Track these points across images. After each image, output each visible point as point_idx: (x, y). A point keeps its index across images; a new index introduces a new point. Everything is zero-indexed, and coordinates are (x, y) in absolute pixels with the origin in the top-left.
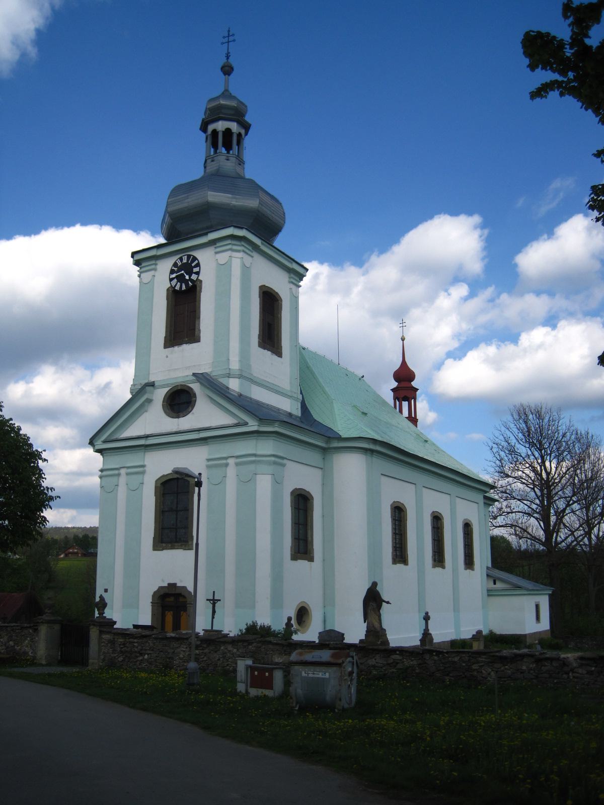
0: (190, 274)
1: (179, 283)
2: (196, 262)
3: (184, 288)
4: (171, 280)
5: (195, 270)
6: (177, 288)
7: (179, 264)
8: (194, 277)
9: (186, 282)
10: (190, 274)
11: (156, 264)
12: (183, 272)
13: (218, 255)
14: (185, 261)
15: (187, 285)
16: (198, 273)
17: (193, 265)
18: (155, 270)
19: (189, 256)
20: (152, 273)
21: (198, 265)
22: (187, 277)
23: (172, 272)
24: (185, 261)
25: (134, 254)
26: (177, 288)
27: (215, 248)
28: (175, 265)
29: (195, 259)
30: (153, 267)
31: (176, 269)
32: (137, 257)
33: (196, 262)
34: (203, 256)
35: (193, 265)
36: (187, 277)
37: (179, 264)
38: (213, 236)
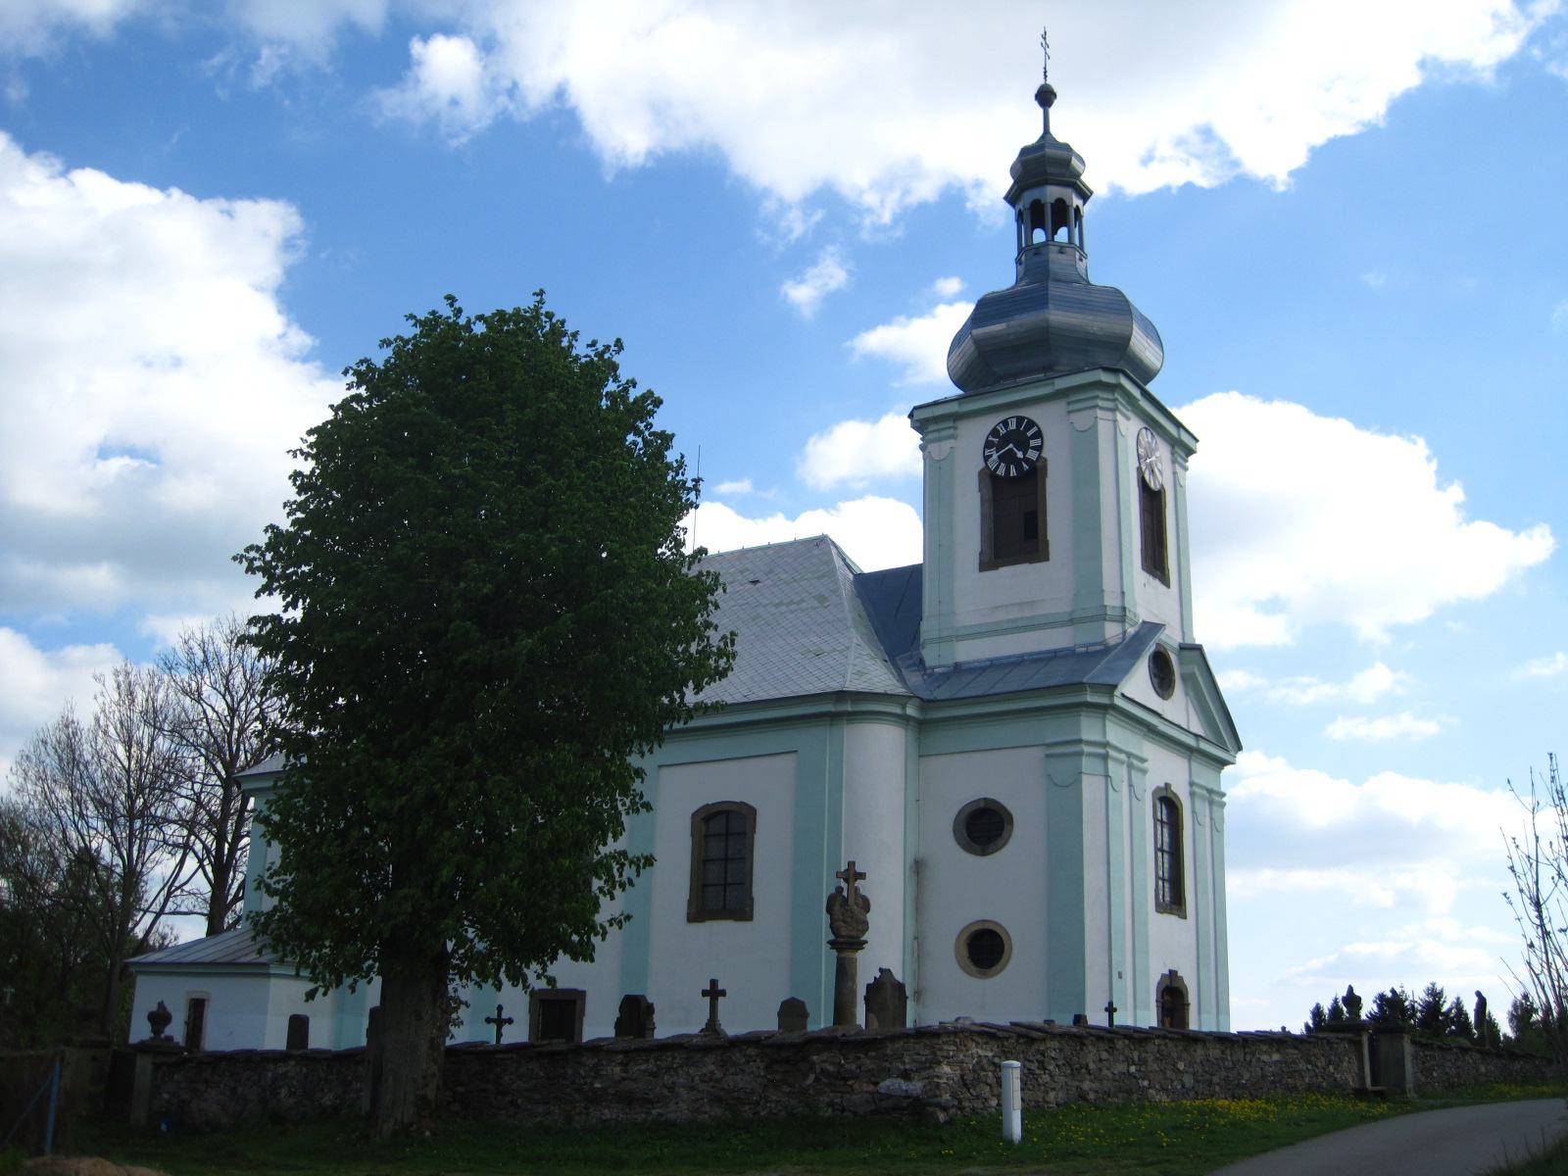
0: (1025, 449)
1: (1002, 464)
2: (1035, 429)
3: (1013, 472)
4: (986, 458)
5: (1033, 443)
6: (1001, 471)
7: (1003, 431)
8: (1032, 455)
9: (1018, 463)
10: (1025, 449)
11: (955, 428)
12: (1011, 446)
13: (1074, 417)
14: (1013, 426)
15: (1019, 468)
16: (1039, 448)
17: (1029, 434)
18: (953, 437)
19: (1020, 419)
20: (947, 445)
21: (1039, 435)
22: (1020, 455)
23: (988, 445)
24: (1013, 426)
26: (1001, 471)
27: (1069, 403)
28: (994, 432)
29: (1031, 424)
30: (951, 431)
31: (996, 440)
32: (918, 415)
33: (1035, 429)
34: (1050, 420)
35: (1029, 434)
36: (1020, 455)
37: (1003, 431)
38: (1062, 383)
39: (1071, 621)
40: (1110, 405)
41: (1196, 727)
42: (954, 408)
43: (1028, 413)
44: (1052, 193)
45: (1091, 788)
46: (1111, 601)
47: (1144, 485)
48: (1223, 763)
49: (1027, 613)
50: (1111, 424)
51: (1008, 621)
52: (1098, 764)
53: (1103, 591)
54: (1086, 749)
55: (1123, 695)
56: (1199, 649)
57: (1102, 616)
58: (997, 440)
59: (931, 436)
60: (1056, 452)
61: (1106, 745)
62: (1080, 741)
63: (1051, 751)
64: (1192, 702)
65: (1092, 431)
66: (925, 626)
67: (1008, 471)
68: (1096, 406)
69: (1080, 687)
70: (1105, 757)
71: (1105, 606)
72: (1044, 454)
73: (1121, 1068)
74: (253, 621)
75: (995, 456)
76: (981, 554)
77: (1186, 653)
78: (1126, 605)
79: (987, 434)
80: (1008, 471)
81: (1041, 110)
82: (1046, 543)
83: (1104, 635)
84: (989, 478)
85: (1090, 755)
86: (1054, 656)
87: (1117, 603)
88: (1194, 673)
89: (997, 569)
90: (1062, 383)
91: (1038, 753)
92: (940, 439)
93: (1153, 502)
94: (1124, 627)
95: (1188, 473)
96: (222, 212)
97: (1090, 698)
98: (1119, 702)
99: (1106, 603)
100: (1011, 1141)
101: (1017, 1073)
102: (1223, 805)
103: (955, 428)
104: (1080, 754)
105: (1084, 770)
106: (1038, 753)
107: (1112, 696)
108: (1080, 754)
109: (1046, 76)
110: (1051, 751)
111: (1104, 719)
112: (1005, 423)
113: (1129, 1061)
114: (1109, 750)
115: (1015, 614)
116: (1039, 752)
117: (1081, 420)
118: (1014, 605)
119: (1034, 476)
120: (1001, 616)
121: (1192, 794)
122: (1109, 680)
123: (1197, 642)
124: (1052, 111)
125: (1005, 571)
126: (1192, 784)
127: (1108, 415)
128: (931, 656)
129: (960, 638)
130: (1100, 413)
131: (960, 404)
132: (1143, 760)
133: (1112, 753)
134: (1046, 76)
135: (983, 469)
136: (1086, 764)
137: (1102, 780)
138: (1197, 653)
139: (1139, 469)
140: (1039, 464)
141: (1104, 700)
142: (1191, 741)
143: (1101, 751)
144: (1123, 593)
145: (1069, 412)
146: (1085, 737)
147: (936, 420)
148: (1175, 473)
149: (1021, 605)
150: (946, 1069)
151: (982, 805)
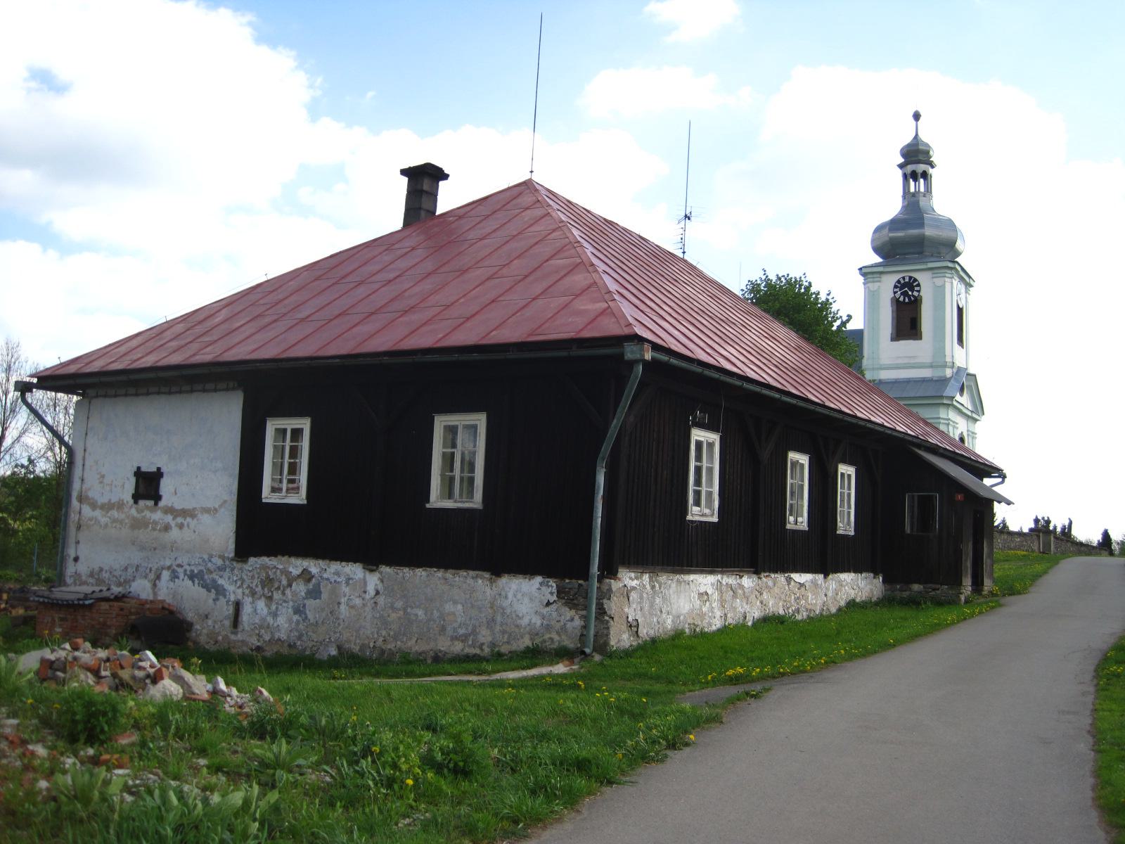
0: (913, 291)
3: (907, 300)
4: (895, 293)
5: (916, 289)
6: (901, 299)
7: (902, 282)
8: (916, 294)
9: (909, 297)
10: (913, 291)
14: (907, 280)
15: (910, 299)
16: (919, 291)
17: (914, 284)
18: (880, 281)
19: (910, 278)
20: (878, 284)
21: (919, 285)
22: (910, 293)
23: (895, 287)
24: (907, 280)
25: (860, 269)
26: (901, 299)
27: (933, 274)
28: (899, 282)
29: (915, 280)
30: (879, 279)
31: (899, 285)
32: (864, 270)
33: (917, 282)
34: (924, 279)
35: (914, 284)
36: (910, 293)
37: (902, 282)
38: (931, 265)
40: (949, 275)
42: (881, 269)
44: (921, 168)
46: (948, 359)
48: (976, 420)
49: (912, 361)
51: (905, 364)
54: (942, 421)
57: (945, 366)
58: (900, 285)
61: (949, 419)
62: (939, 418)
65: (943, 286)
66: (865, 362)
67: (904, 299)
68: (945, 277)
69: (942, 397)
70: (948, 424)
75: (899, 293)
77: (969, 377)
80: (904, 299)
81: (914, 122)
85: (943, 423)
90: (931, 265)
92: (874, 282)
93: (960, 311)
97: (945, 402)
98: (955, 403)
102: (976, 438)
103: (880, 277)
104: (940, 423)
108: (940, 423)
112: (904, 278)
115: (906, 361)
117: (938, 282)
119: (916, 303)
120: (900, 361)
121: (968, 435)
125: (902, 342)
126: (968, 431)
130: (947, 279)
132: (957, 424)
133: (951, 423)
138: (974, 377)
140: (919, 298)
141: (950, 402)
142: (969, 413)
143: (947, 422)
144: (953, 356)
145: (933, 278)
148: (966, 298)
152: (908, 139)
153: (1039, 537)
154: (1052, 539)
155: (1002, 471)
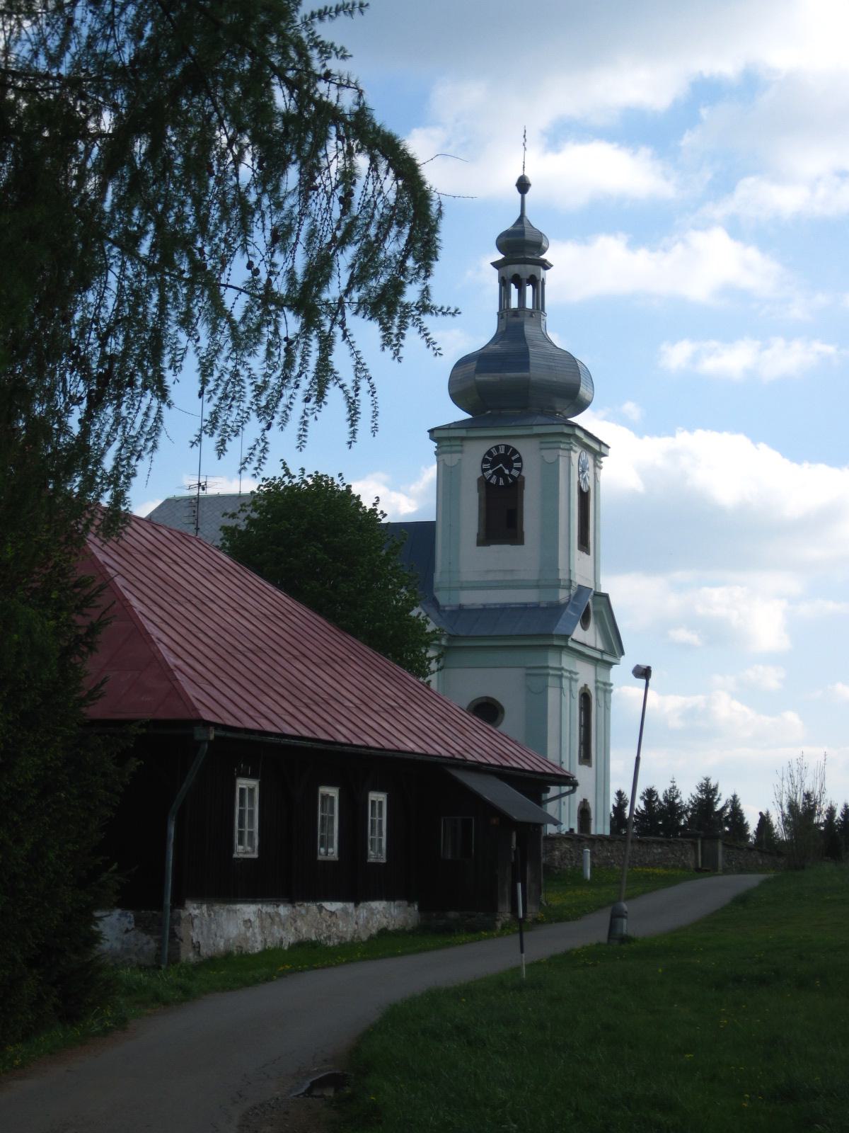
0: (510, 468)
1: (495, 476)
2: (517, 456)
3: (501, 482)
4: (484, 470)
5: (516, 465)
7: (495, 454)
8: (515, 473)
10: (510, 468)
11: (462, 446)
12: (501, 465)
13: (544, 453)
14: (502, 451)
15: (506, 480)
16: (520, 469)
17: (513, 458)
18: (461, 452)
19: (507, 447)
20: (457, 456)
21: (519, 460)
22: (507, 472)
23: (485, 461)
24: (502, 451)
25: (431, 431)
26: (493, 481)
27: (542, 443)
28: (489, 453)
29: (515, 452)
32: (437, 434)
33: (517, 456)
34: (526, 449)
35: (513, 458)
36: (507, 472)
38: (537, 430)
39: (538, 587)
40: (567, 447)
41: (600, 646)
42: (463, 433)
43: (515, 444)
44: (525, 270)
45: (552, 694)
46: (562, 575)
47: (580, 490)
48: (610, 665)
49: (509, 577)
50: (566, 459)
51: (497, 581)
52: (556, 681)
53: (558, 569)
54: (551, 672)
55: (572, 639)
56: (606, 596)
57: (556, 585)
58: (491, 460)
59: (444, 449)
60: (531, 472)
61: (562, 669)
62: (547, 667)
63: (530, 672)
64: (599, 632)
65: (556, 463)
66: (438, 577)
67: (498, 481)
68: (560, 448)
69: (551, 636)
70: (561, 677)
71: (560, 580)
72: (523, 473)
73: (605, 854)
74: (111, 622)
75: (490, 472)
76: (478, 535)
77: (597, 598)
78: (572, 579)
79: (485, 453)
80: (498, 481)
81: (520, 195)
82: (522, 533)
83: (558, 597)
84: (484, 484)
85: (553, 675)
86: (525, 608)
87: (566, 577)
88: (602, 612)
89: (489, 545)
90: (537, 430)
91: (522, 672)
92: (451, 452)
93: (584, 497)
94: (570, 592)
95: (602, 471)
96: (162, 421)
97: (556, 643)
98: (571, 644)
99: (560, 577)
100: (586, 880)
101: (589, 854)
102: (611, 691)
103: (462, 446)
104: (548, 675)
105: (549, 685)
106: (522, 672)
107: (567, 641)
108: (548, 675)
109: (524, 170)
110: (530, 672)
111: (561, 653)
112: (497, 448)
113: (608, 851)
114: (563, 672)
115: (499, 577)
116: (522, 671)
117: (549, 455)
118: (500, 571)
119: (515, 488)
120: (490, 577)
121: (597, 688)
122: (567, 633)
123: (603, 591)
124: (527, 196)
125: (494, 548)
126: (596, 681)
127: (565, 453)
128: (442, 597)
129: (462, 588)
130: (561, 452)
131: (467, 431)
132: (576, 674)
133: (566, 674)
134: (524, 170)
135: (481, 477)
136: (550, 680)
137: (558, 689)
138: (605, 599)
139: (579, 482)
140: (519, 480)
141: (562, 643)
142: (598, 655)
143: (559, 673)
144: (570, 571)
145: (541, 449)
146: (551, 664)
147: (450, 439)
148: (595, 474)
149: (505, 571)
150: (557, 853)
151: (484, 701)
152: (508, 224)
153: (695, 845)
154: (720, 847)
155: (573, 778)
